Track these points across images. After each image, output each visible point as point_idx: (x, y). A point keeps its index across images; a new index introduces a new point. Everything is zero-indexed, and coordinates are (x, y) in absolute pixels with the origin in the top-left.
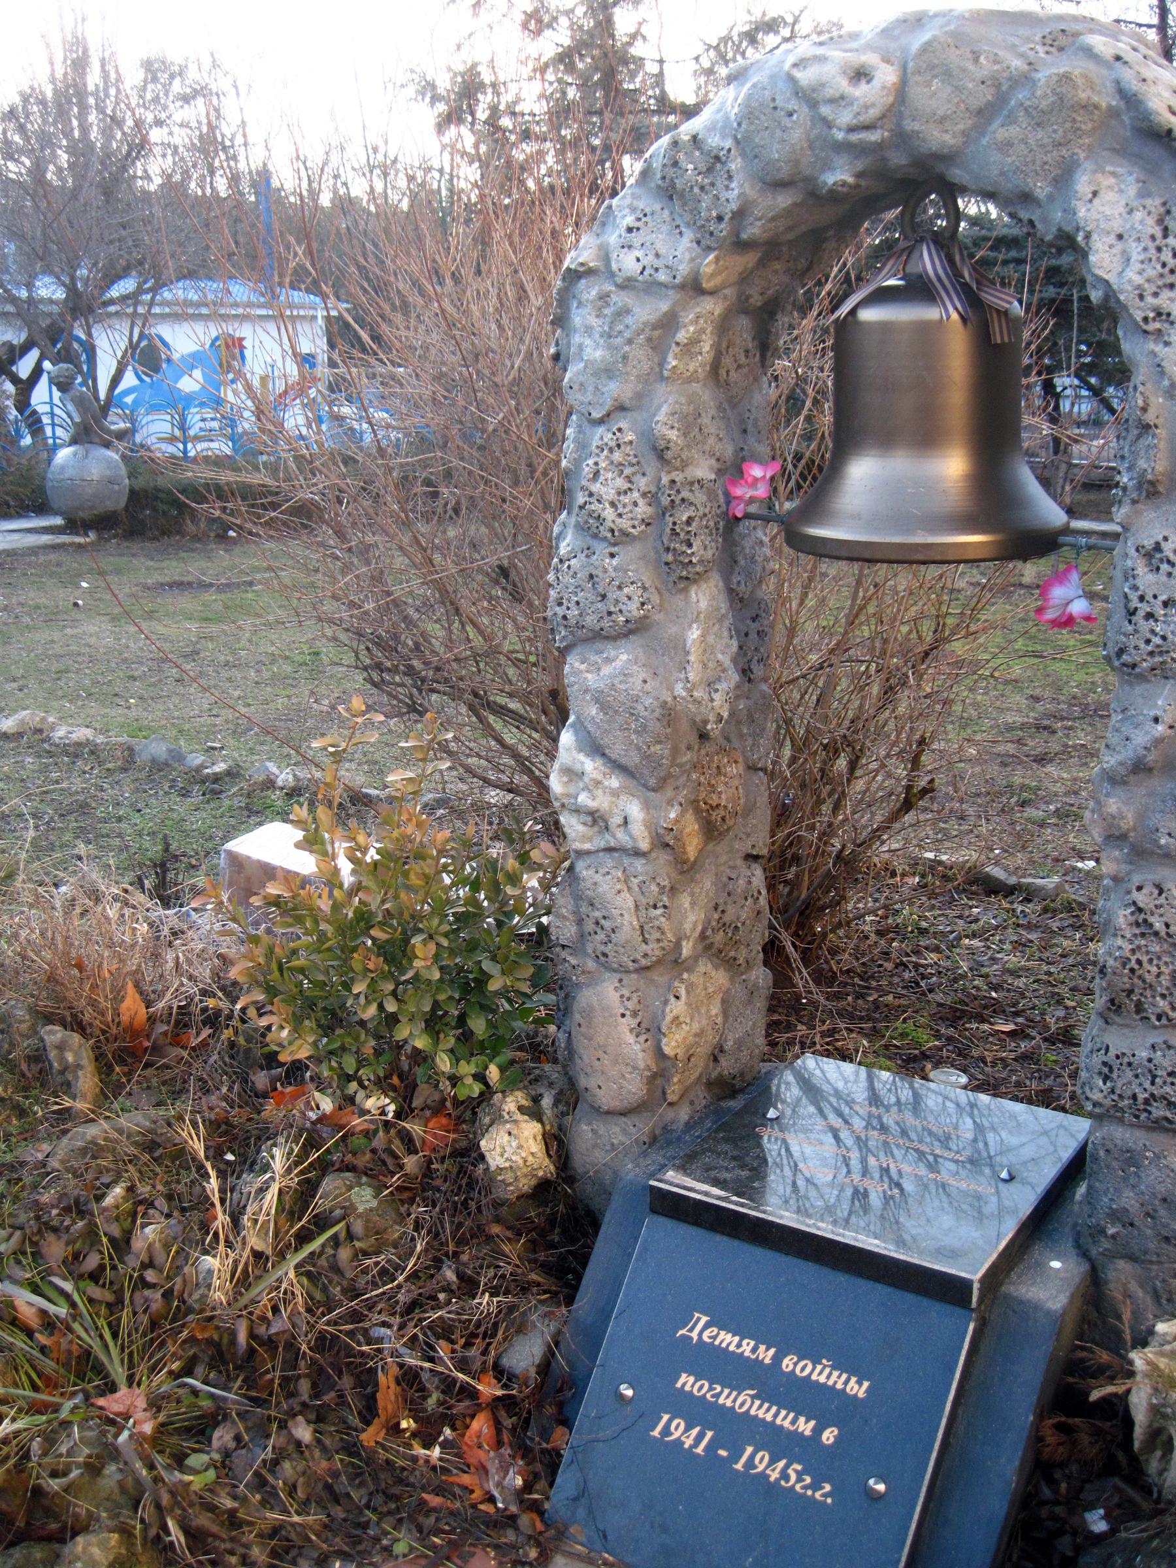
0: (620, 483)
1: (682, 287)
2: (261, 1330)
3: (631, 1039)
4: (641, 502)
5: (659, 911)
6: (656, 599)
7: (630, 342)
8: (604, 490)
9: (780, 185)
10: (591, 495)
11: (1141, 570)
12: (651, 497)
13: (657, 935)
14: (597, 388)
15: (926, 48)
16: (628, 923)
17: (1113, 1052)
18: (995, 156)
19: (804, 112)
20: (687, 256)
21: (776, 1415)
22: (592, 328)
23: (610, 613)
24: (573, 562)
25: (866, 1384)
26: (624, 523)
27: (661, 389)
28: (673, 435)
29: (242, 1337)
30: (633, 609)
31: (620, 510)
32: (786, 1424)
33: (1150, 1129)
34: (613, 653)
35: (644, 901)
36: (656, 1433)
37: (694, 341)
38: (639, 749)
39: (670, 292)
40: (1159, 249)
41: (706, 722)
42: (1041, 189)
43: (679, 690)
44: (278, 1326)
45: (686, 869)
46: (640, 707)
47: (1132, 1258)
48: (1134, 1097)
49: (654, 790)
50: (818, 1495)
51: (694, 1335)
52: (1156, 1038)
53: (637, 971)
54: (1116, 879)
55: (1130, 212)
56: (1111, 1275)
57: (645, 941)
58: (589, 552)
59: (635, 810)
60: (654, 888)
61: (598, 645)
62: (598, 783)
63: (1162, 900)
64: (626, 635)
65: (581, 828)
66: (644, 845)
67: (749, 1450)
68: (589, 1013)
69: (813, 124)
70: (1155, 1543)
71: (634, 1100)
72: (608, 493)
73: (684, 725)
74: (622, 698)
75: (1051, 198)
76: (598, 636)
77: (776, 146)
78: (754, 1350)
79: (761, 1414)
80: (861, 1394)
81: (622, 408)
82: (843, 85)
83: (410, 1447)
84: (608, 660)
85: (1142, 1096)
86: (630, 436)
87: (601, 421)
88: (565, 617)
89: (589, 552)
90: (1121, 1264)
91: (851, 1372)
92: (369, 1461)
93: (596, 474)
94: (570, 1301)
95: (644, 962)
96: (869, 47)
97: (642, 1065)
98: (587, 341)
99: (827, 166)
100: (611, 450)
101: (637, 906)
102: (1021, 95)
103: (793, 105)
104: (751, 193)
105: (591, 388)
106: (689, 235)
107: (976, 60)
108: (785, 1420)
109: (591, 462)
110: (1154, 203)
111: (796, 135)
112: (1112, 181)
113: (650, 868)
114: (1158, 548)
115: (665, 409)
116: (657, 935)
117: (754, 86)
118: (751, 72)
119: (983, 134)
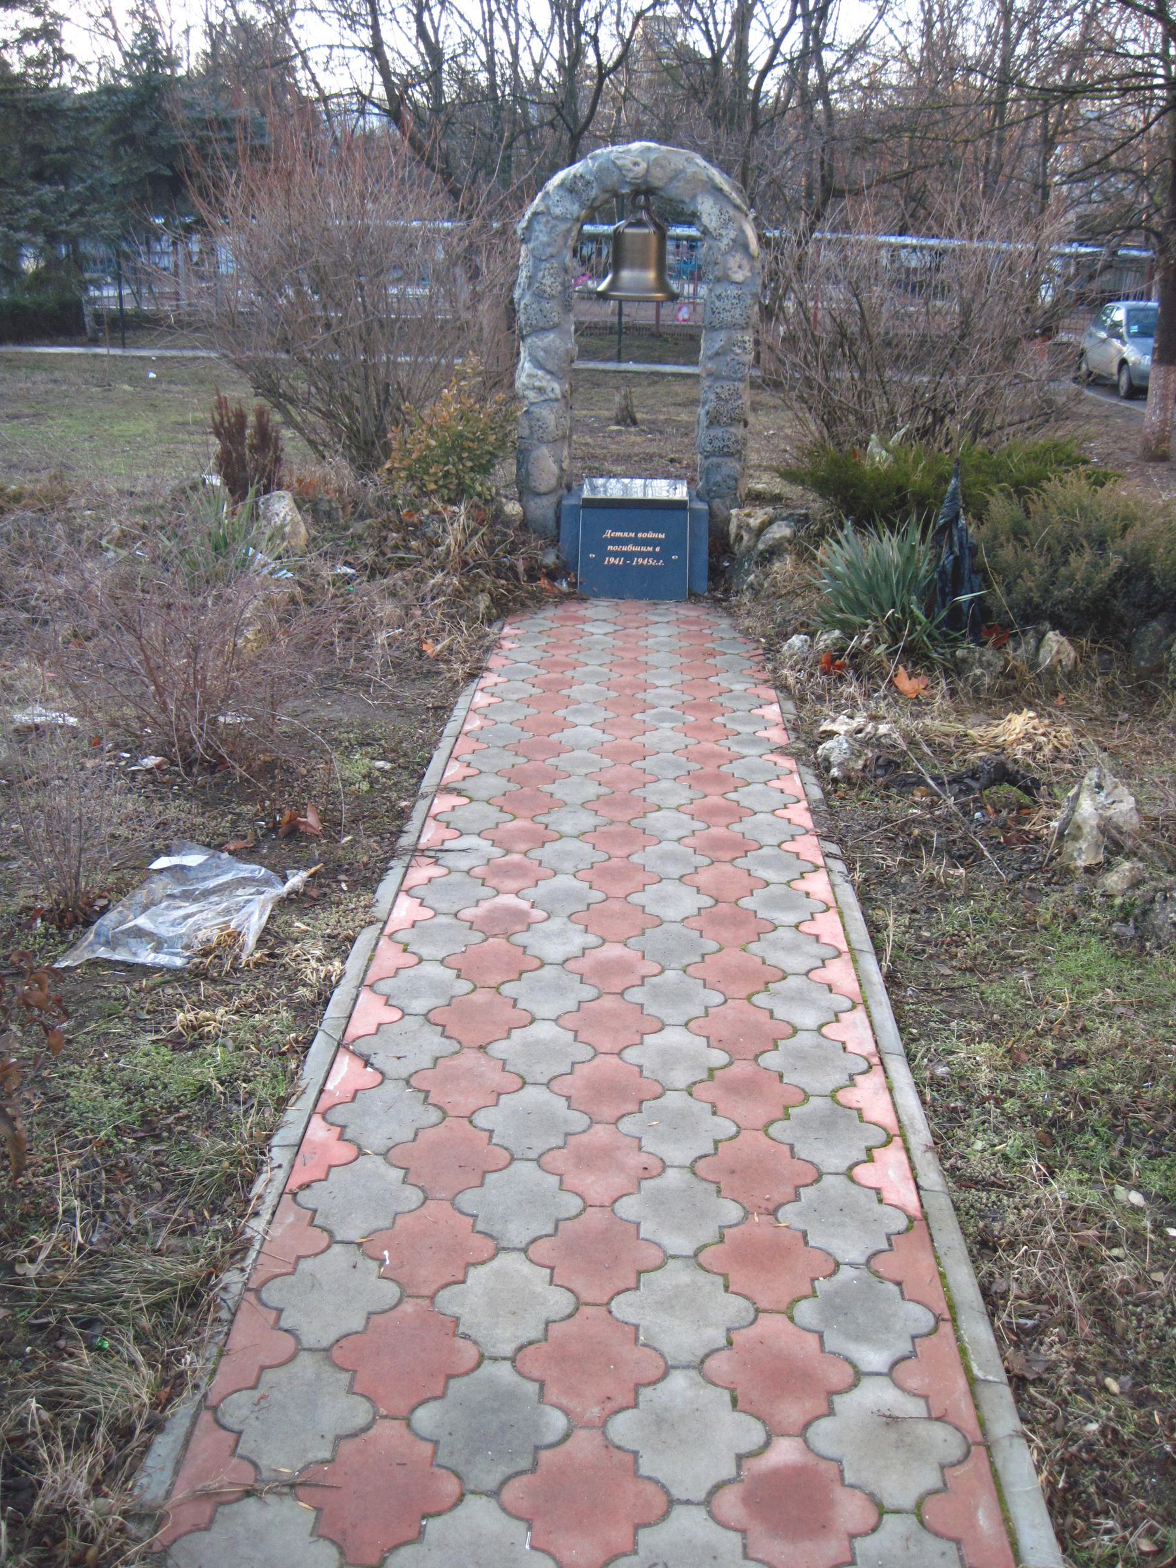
12: (563, 284)
16: (552, 424)
19: (616, 172)
42: (687, 200)
59: (556, 386)
108: (644, 549)
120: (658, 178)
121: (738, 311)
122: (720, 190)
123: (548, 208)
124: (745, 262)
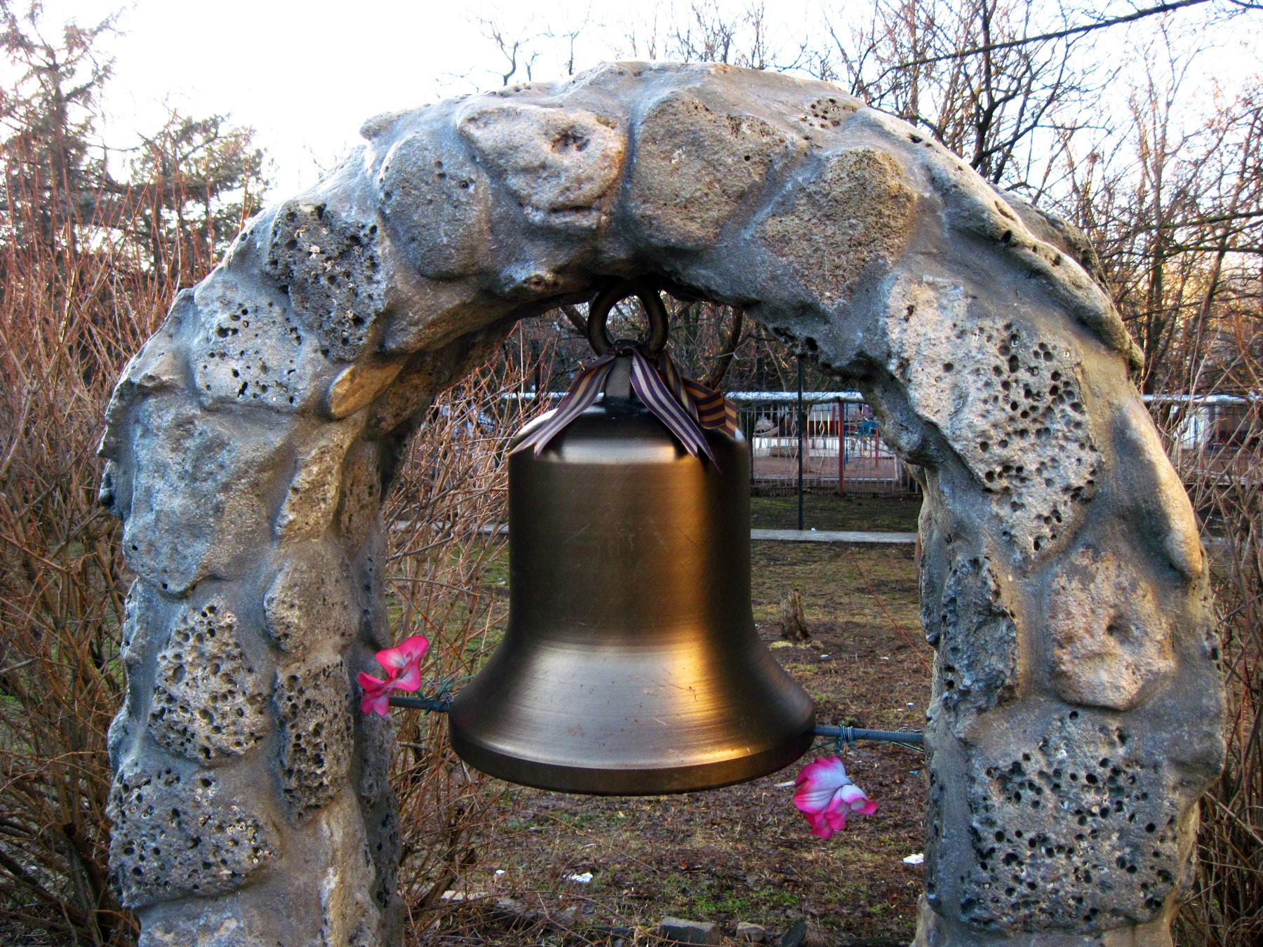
0: (217, 684)
1: (302, 412)
4: (248, 710)
6: (274, 840)
7: (226, 487)
8: (191, 693)
10: (171, 699)
11: (996, 799)
12: (265, 702)
14: (175, 550)
15: (664, 108)
18: (763, 254)
19: (483, 182)
20: (309, 370)
23: (207, 865)
24: (146, 790)
26: (224, 740)
27: (272, 553)
28: (293, 616)
30: (243, 858)
31: (218, 721)
34: (214, 919)
37: (318, 484)
39: (285, 420)
40: (1006, 385)
42: (830, 300)
55: (962, 334)
61: (189, 907)
69: (497, 201)
72: (199, 698)
75: (843, 312)
76: (189, 895)
77: (444, 227)
82: (545, 150)
84: (208, 929)
86: (229, 618)
87: (183, 596)
88: (137, 871)
93: (178, 671)
96: (576, 103)
98: (159, 484)
99: (515, 256)
100: (200, 638)
103: (467, 172)
104: (405, 288)
105: (166, 550)
106: (311, 343)
107: (736, 129)
109: (170, 653)
111: (475, 213)
112: (930, 294)
114: (1017, 768)
115: (280, 580)
117: (408, 144)
119: (744, 224)
120: (681, 203)
121: (1109, 846)
122: (1001, 243)
123: (186, 368)
124: (1145, 604)
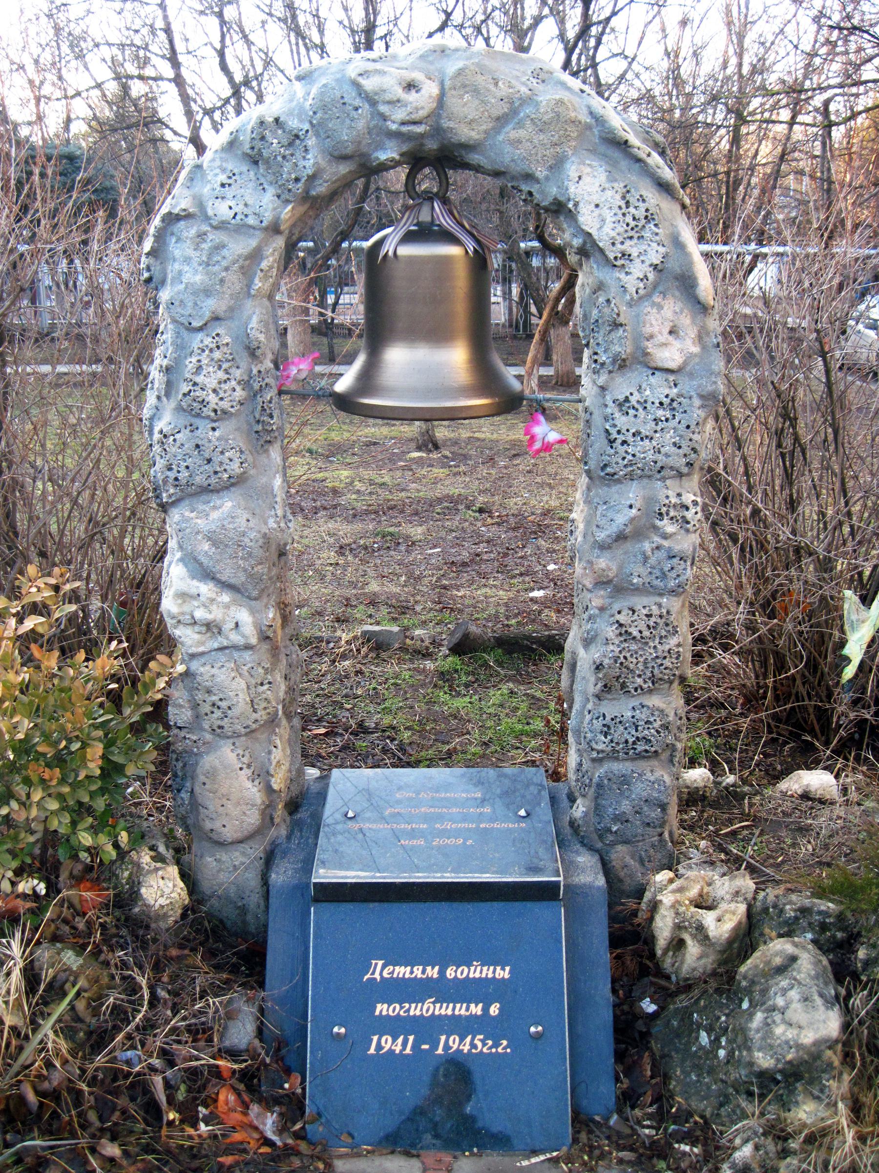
0: (221, 375)
1: (266, 229)
2: (46, 1085)
3: (249, 784)
4: (238, 388)
5: (266, 687)
6: (250, 459)
7: (227, 269)
8: (207, 380)
9: (344, 158)
10: (195, 384)
11: (617, 415)
12: (246, 384)
13: (264, 704)
14: (196, 304)
15: (460, 72)
16: (243, 699)
17: (608, 718)
18: (508, 149)
20: (271, 206)
21: (454, 1009)
22: (190, 258)
23: (216, 473)
24: (178, 436)
25: (508, 969)
26: (225, 405)
27: (249, 303)
28: (262, 337)
29: (31, 1097)
30: (235, 468)
31: (222, 395)
32: (463, 1012)
33: (633, 760)
34: (218, 502)
35: (254, 682)
36: (372, 1051)
37: (271, 267)
38: (245, 570)
39: (257, 233)
40: (624, 215)
41: (285, 545)
42: (541, 172)
43: (272, 523)
44: (57, 1078)
45: (275, 651)
46: (246, 540)
47: (626, 842)
48: (627, 742)
49: (256, 599)
50: (500, 1050)
51: (377, 976)
52: (635, 702)
53: (246, 734)
54: (602, 609)
55: (603, 190)
56: (613, 856)
57: (255, 711)
58: (194, 429)
59: (244, 616)
60: (261, 670)
61: (204, 497)
62: (212, 600)
63: (635, 617)
64: (227, 488)
65: (197, 637)
66: (254, 641)
67: (443, 1038)
68: (212, 774)
69: (372, 118)
70: (702, 1003)
71: (251, 829)
72: (211, 382)
73: (273, 547)
74: (231, 535)
75: (547, 178)
76: (207, 490)
77: (345, 131)
78: (423, 972)
79: (443, 1012)
80: (507, 976)
81: (216, 318)
82: (399, 93)
83: (183, 1130)
84: (215, 508)
85: (631, 740)
86: (227, 340)
87: (200, 329)
88: (176, 479)
89: (194, 429)
90: (619, 848)
91: (495, 964)
92: (168, 1152)
93: (199, 368)
94: (262, 985)
95: (254, 726)
96: (413, 68)
97: (259, 801)
98: (186, 268)
99: (380, 147)
100: (211, 350)
101: (248, 688)
102: (528, 110)
103: (358, 102)
104: (323, 163)
105: (190, 304)
106: (271, 191)
107: (496, 84)
108: (461, 1010)
109: (194, 359)
110: (619, 186)
111: (361, 125)
112: (588, 170)
113: (255, 657)
114: (627, 400)
115: (255, 319)
116: (264, 704)
117: (325, 86)
118: (316, 74)
119: (499, 133)
120: (467, 122)
121: (669, 437)
122: (623, 145)
123: (201, 206)
124: (686, 321)
